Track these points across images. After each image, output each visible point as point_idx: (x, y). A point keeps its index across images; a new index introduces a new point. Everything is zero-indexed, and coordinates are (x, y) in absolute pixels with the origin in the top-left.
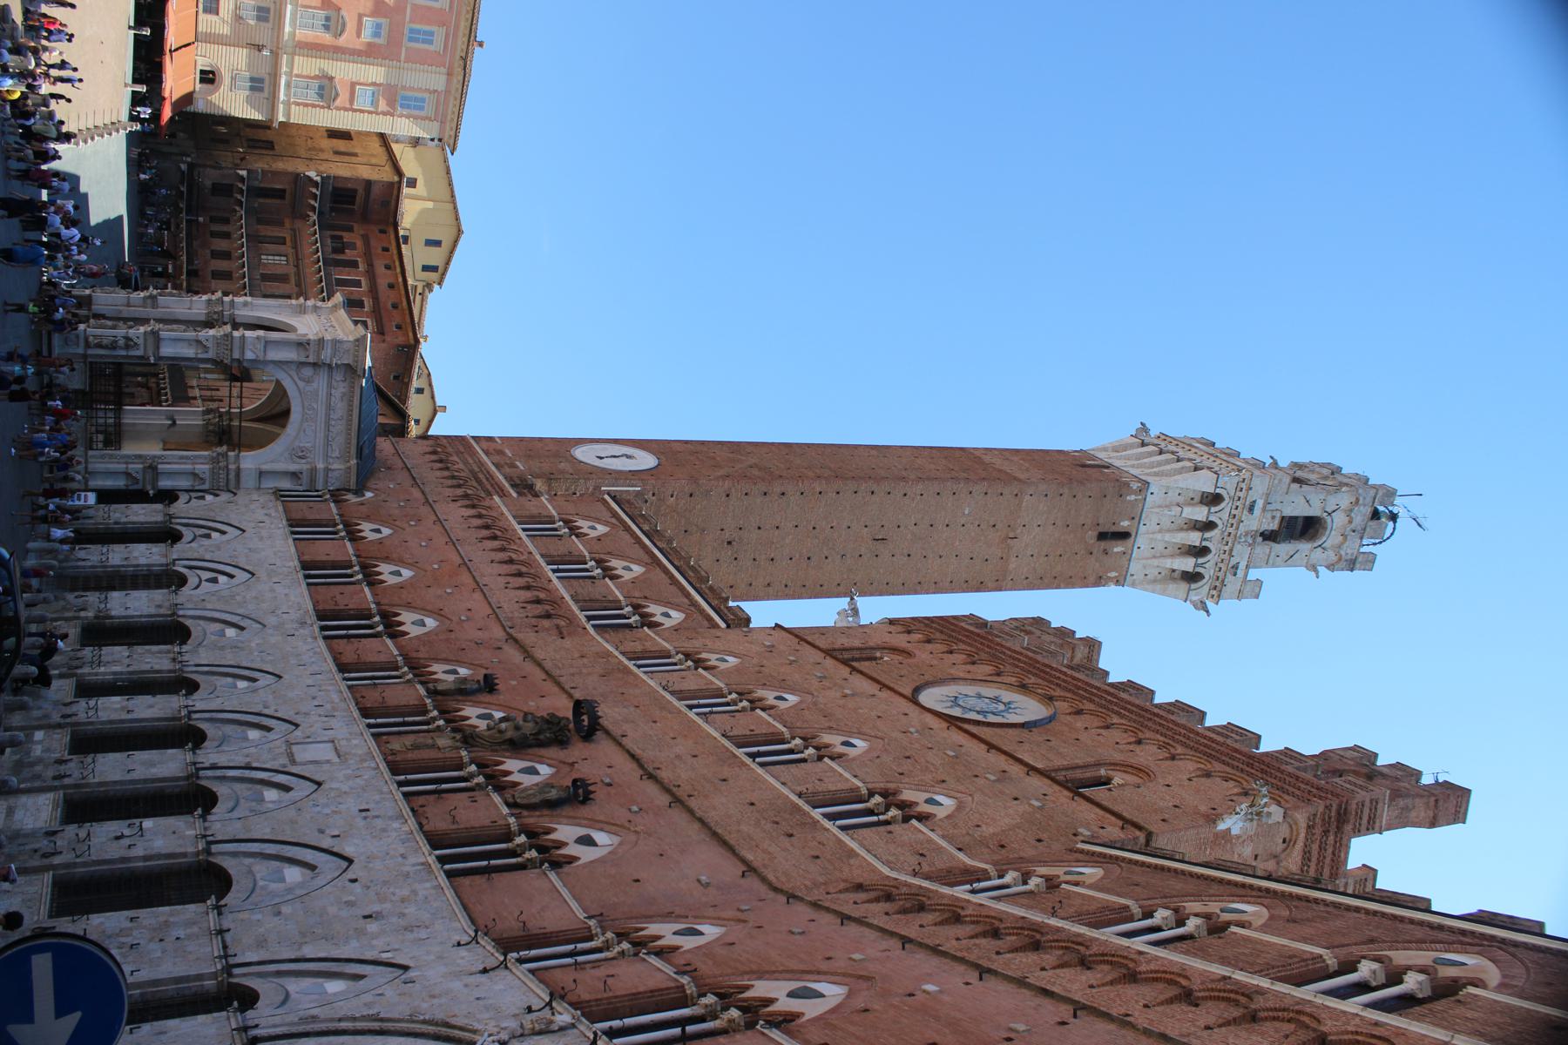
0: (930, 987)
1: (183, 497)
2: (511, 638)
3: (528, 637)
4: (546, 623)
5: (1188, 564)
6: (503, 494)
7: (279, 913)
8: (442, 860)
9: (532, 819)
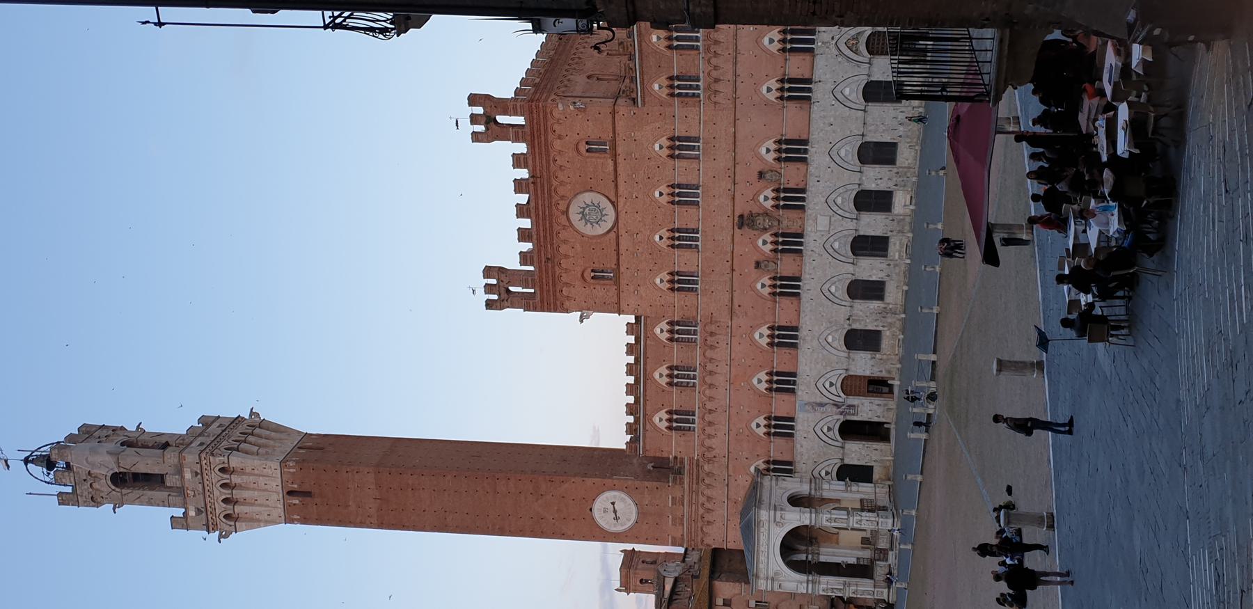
1: (834, 474)
2: (732, 311)
3: (724, 318)
4: (713, 328)
5: (257, 431)
6: (691, 459)
8: (806, 151)
9: (776, 165)
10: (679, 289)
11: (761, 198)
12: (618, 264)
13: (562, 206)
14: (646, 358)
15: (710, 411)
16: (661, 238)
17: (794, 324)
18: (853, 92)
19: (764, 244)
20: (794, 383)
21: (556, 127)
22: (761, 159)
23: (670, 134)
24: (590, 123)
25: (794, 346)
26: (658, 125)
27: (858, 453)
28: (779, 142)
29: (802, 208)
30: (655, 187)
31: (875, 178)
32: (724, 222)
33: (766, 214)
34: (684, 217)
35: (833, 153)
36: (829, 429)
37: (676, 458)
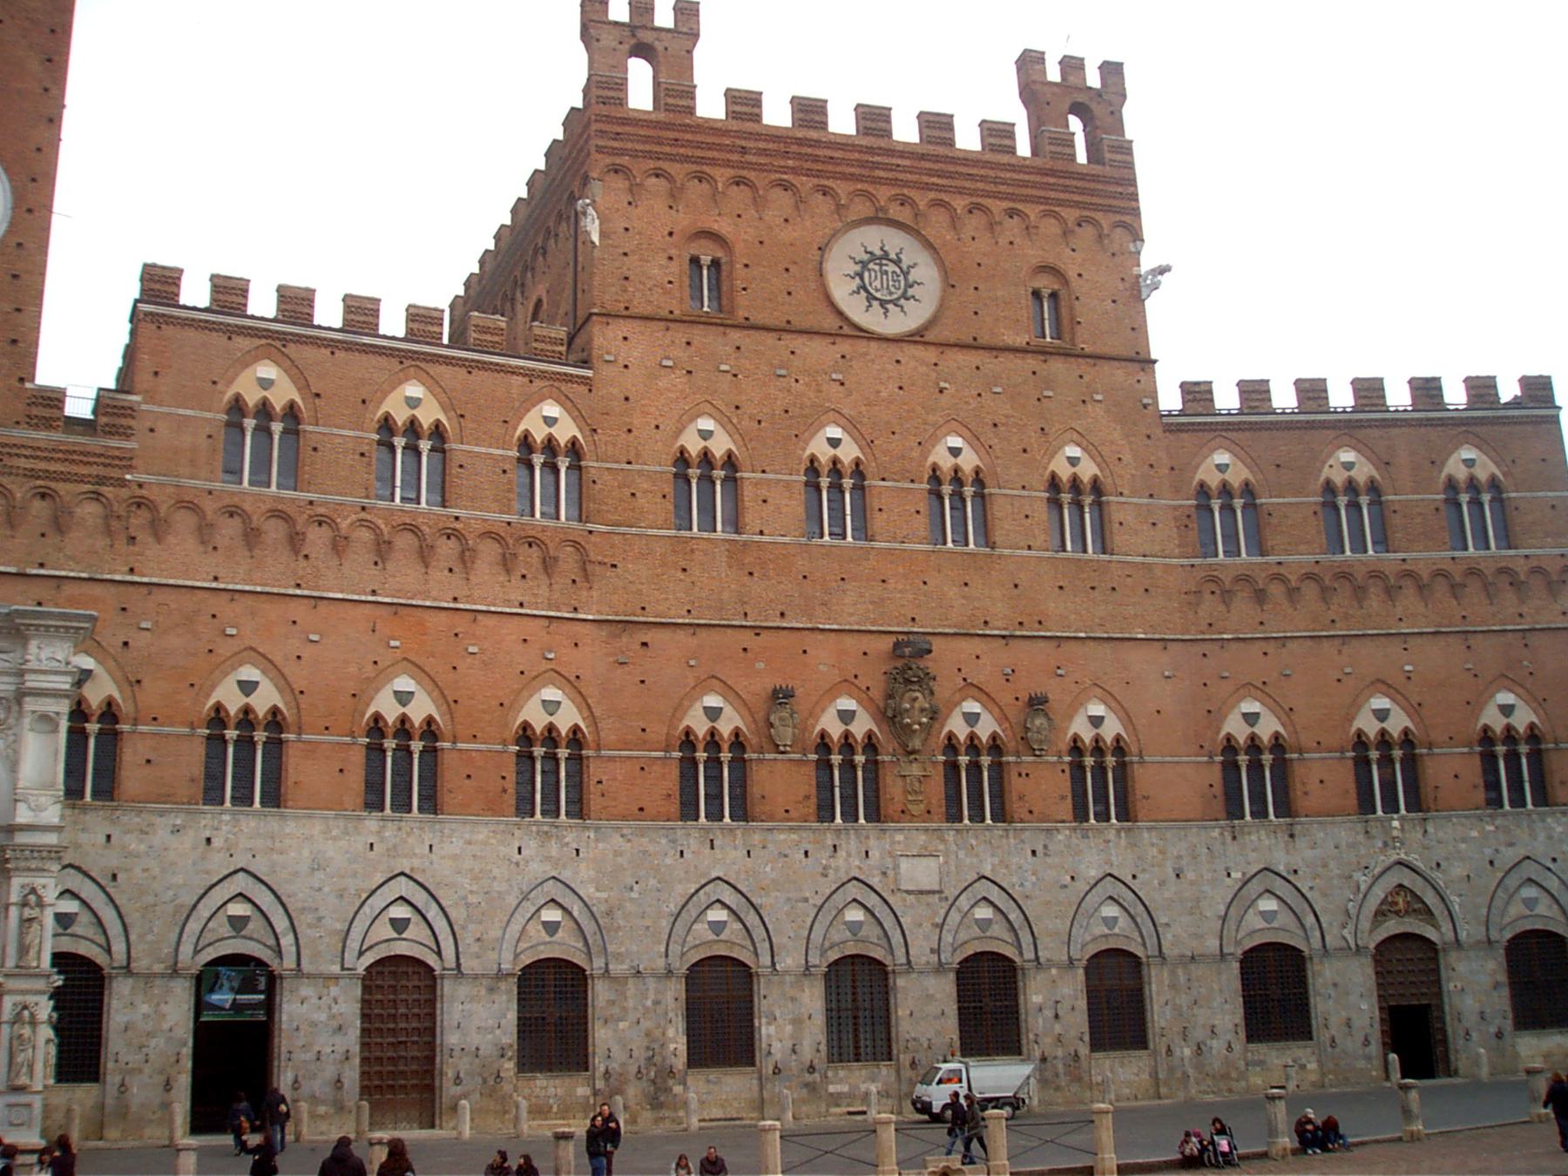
0: (1408, 668)
1: (67, 945)
6: (126, 461)
7: (1167, 925)
8: (1103, 816)
10: (682, 478)
11: (975, 707)
12: (748, 326)
13: (895, 211)
14: (470, 366)
15: (295, 541)
16: (834, 443)
17: (594, 801)
18: (1266, 918)
19: (843, 715)
20: (402, 805)
21: (1088, 232)
22: (1077, 704)
23: (1107, 482)
24: (1109, 305)
25: (524, 807)
26: (1127, 457)
27: (152, 1028)
28: (1119, 748)
29: (954, 816)
30: (975, 439)
31: (1054, 1002)
32: (905, 606)
33: (935, 715)
34: (899, 508)
35: (1109, 887)
36: (238, 923)
37: (129, 411)
